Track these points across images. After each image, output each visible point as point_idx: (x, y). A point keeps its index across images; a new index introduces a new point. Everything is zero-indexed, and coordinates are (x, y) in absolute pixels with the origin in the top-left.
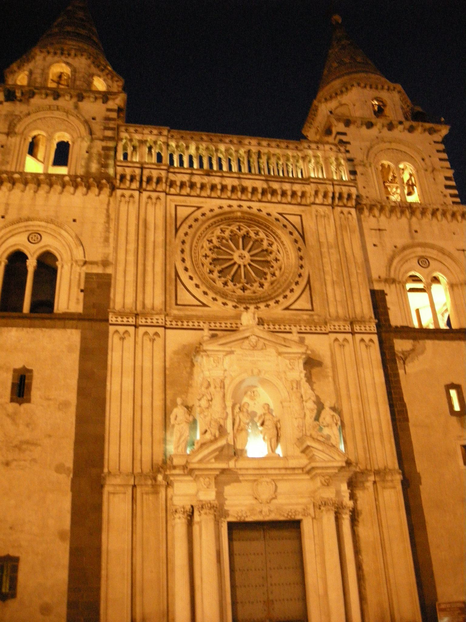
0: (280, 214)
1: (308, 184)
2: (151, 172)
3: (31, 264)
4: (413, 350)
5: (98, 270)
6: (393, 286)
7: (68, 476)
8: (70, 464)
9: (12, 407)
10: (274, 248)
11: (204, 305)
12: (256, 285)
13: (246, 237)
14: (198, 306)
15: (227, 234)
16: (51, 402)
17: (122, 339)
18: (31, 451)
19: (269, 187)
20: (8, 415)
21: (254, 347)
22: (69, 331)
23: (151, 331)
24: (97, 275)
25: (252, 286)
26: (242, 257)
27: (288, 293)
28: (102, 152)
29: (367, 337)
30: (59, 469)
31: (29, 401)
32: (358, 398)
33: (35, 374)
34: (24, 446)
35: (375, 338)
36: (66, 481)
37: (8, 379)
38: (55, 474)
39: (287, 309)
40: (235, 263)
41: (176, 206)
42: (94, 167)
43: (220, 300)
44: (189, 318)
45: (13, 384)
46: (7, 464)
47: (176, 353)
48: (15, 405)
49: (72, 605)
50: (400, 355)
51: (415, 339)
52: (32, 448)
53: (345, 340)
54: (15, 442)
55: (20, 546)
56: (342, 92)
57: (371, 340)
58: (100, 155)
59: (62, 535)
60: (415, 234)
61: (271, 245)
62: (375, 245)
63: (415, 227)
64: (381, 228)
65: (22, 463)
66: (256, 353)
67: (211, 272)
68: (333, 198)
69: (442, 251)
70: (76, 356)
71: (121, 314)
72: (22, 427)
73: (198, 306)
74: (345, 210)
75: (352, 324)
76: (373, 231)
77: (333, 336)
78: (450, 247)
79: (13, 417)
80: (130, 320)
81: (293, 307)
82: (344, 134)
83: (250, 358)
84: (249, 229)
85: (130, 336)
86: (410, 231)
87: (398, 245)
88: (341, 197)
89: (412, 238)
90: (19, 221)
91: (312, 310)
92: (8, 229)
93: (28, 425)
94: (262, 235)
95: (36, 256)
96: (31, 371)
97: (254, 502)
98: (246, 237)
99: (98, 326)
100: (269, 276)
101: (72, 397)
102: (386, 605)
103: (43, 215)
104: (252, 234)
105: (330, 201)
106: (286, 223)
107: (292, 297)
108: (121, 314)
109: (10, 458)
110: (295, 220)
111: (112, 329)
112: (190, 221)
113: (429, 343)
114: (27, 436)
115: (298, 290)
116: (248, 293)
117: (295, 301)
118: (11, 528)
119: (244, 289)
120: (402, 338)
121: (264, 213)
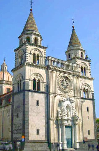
8: (44, 116)
21: (68, 101)
30: (43, 116)
31: (39, 106)
37: (36, 102)
46: (37, 115)
79: (37, 108)
103: (38, 72)
107: (71, 92)
111: (50, 95)
119: (65, 89)
121: (68, 76)
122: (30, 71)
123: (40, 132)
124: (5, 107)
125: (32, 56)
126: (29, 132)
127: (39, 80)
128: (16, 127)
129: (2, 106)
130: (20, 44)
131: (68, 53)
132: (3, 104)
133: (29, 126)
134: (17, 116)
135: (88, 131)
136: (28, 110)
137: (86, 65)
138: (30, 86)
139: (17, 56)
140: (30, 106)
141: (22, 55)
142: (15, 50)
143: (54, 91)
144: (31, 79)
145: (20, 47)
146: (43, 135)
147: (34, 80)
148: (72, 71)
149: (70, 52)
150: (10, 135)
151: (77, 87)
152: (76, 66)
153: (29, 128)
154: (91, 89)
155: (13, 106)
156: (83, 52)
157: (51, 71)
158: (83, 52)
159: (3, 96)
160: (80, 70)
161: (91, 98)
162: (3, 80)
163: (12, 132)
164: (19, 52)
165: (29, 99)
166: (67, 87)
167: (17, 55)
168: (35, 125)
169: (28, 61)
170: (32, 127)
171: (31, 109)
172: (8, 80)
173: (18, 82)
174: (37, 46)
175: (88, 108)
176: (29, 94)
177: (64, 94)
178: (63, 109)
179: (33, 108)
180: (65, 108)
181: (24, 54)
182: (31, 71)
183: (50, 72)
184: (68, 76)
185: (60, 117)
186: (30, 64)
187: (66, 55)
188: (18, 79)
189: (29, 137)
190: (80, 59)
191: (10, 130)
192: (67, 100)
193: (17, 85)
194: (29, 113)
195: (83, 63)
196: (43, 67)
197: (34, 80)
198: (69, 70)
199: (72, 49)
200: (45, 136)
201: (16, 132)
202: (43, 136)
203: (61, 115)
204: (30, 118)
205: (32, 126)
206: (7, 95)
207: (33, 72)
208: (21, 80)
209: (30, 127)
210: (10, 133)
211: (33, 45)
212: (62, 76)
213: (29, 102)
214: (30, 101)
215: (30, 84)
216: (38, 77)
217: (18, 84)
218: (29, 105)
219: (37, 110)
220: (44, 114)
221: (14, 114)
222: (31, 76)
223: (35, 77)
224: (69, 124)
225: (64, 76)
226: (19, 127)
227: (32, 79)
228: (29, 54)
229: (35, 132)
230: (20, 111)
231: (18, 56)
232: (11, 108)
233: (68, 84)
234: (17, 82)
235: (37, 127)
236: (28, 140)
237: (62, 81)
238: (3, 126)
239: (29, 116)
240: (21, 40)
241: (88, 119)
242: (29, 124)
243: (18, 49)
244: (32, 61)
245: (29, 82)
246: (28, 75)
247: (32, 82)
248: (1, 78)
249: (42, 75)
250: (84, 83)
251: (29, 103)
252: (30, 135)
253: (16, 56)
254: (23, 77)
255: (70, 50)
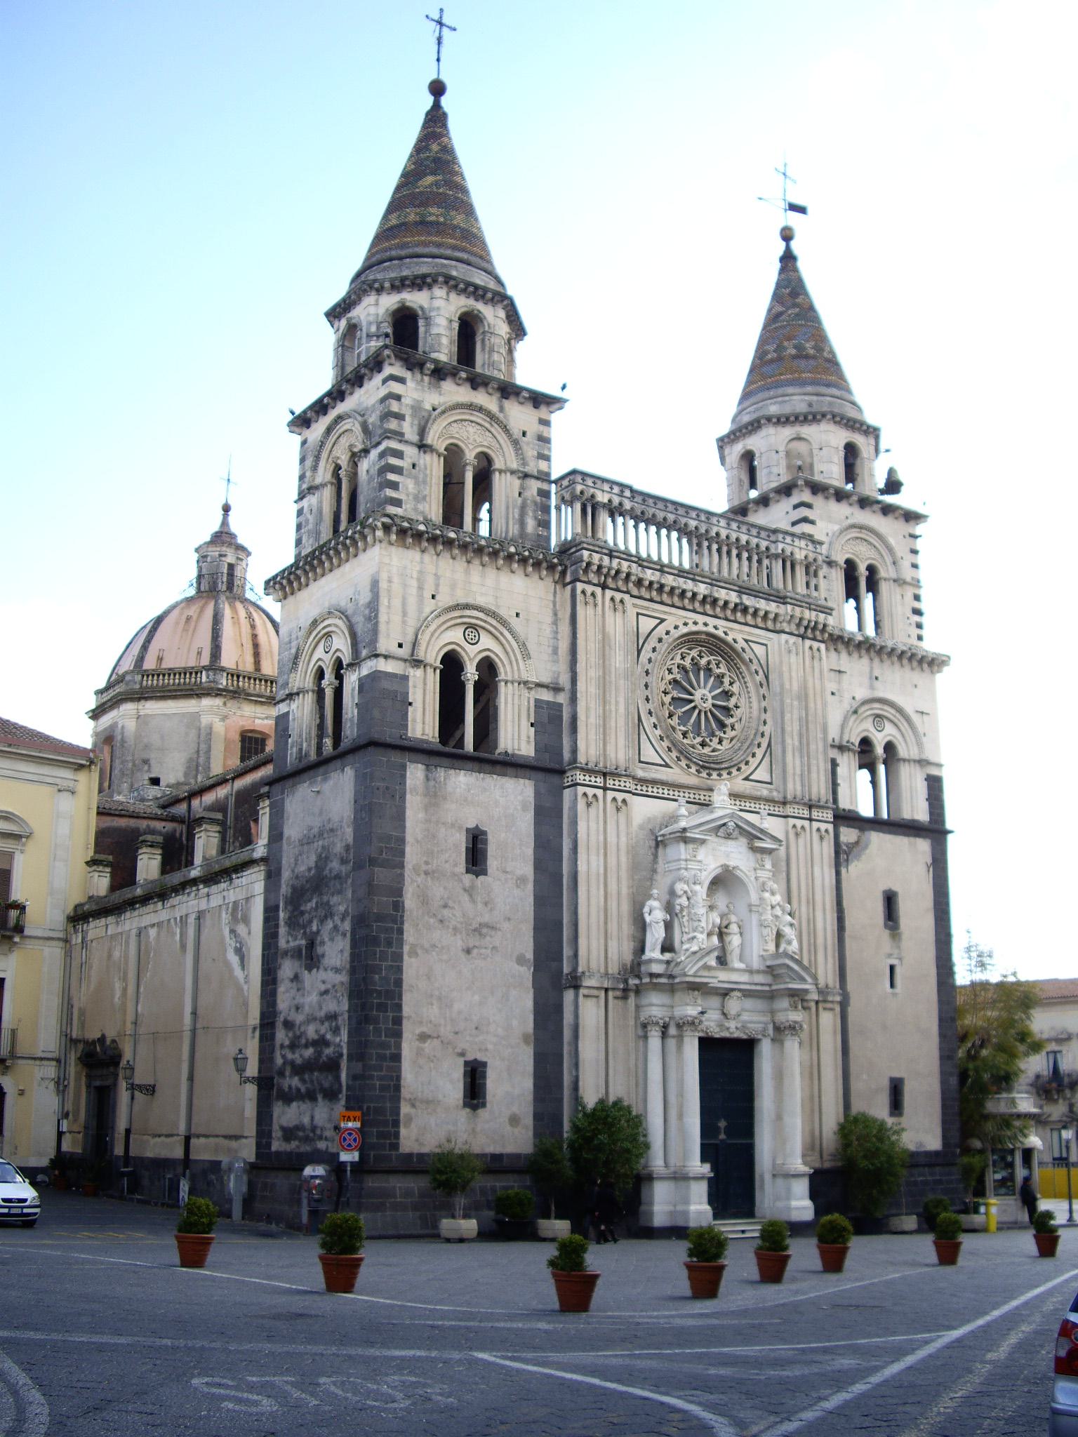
0: (746, 641)
1: (784, 603)
2: (619, 563)
3: (471, 674)
4: (857, 843)
5: (546, 696)
6: (846, 755)
7: (529, 969)
8: (530, 955)
9: (468, 878)
10: (735, 688)
11: (667, 766)
12: (716, 740)
13: (708, 670)
14: (661, 765)
15: (687, 663)
16: (509, 876)
17: (589, 805)
18: (491, 936)
19: (741, 604)
20: (465, 890)
21: (728, 836)
22: (522, 781)
23: (620, 796)
24: (548, 703)
25: (711, 740)
26: (704, 699)
27: (750, 758)
28: (538, 499)
29: (823, 826)
30: (521, 960)
32: (808, 902)
33: (490, 837)
34: (484, 931)
35: (830, 827)
36: (527, 973)
37: (461, 841)
38: (517, 967)
39: (746, 779)
40: (695, 708)
41: (638, 614)
42: (531, 525)
43: (683, 763)
44: (654, 782)
45: (467, 848)
47: (641, 827)
48: (470, 876)
49: (537, 1117)
50: (845, 848)
51: (862, 830)
52: (493, 933)
53: (803, 827)
54: (475, 925)
55: (486, 1050)
56: (806, 419)
57: (827, 831)
58: (535, 503)
59: (525, 1038)
60: (875, 682)
61: (731, 684)
62: (833, 694)
63: (876, 673)
64: (842, 669)
65: (483, 951)
66: (730, 842)
67: (670, 716)
68: (806, 628)
69: (900, 711)
70: (530, 816)
71: (587, 770)
72: (480, 906)
73: (661, 765)
74: (816, 645)
75: (810, 807)
76: (833, 673)
77: (792, 821)
78: (909, 709)
79: (470, 891)
80: (598, 780)
81: (751, 778)
82: (809, 506)
83: (723, 848)
84: (712, 658)
85: (597, 800)
86: (871, 678)
87: (857, 698)
88: (814, 629)
89: (872, 687)
90: (457, 607)
91: (770, 783)
92: (442, 619)
93: (486, 904)
94: (723, 669)
95: (475, 664)
96: (484, 833)
97: (722, 1017)
98: (720, 677)
99: (555, 779)
100: (728, 729)
101: (528, 870)
102: (817, 1133)
103: (481, 601)
104: (726, 680)
105: (802, 630)
106: (752, 657)
107: (754, 762)
108: (587, 770)
109: (471, 945)
110: (759, 650)
112: (652, 642)
113: (876, 839)
114: (486, 918)
115: (759, 753)
116: (706, 750)
117: (756, 769)
118: (477, 1028)
119: (703, 744)
120: (848, 826)
121: (729, 639)
122: (414, 583)
123: (494, 1085)
124: (211, 878)
125: (434, 468)
126: (398, 1088)
127: (488, 668)
128: (293, 1046)
129: (194, 873)
130: (341, 365)
131: (739, 448)
132: (198, 859)
133: (398, 1035)
134: (310, 957)
135: (886, 1084)
136: (398, 906)
137: (890, 549)
138: (415, 714)
139: (315, 468)
140: (408, 872)
141: (354, 455)
142: (302, 422)
143: (619, 754)
144: (420, 654)
145: (337, 394)
146: (515, 1109)
147: (451, 664)
148: (768, 597)
149: (754, 442)
150: (250, 1111)
151: (805, 722)
152: (800, 551)
153: (397, 1058)
154: (920, 744)
155: (273, 877)
156: (859, 440)
157: (589, 589)
158: (859, 440)
159: (209, 798)
160: (833, 583)
161: (921, 813)
162: (214, 665)
163: (267, 1087)
164: (329, 431)
165: (400, 817)
166: (722, 725)
167: (317, 458)
168: (446, 1031)
169: (397, 503)
170: (427, 1046)
171: (424, 900)
172: (248, 666)
173: (320, 674)
174: (476, 382)
175: (890, 900)
176: (404, 777)
177: (692, 780)
178: (684, 901)
179: (437, 891)
180: (701, 891)
181: (366, 451)
182: (420, 588)
183: (580, 597)
184: (736, 634)
185: (657, 968)
186: (418, 536)
187: (723, 460)
188: (320, 652)
189: (396, 1123)
190: (840, 496)
191: (252, 1069)
192: (719, 829)
193: (309, 700)
194: (401, 931)
195: (861, 527)
196: (523, 561)
197: (451, 664)
198: (742, 590)
199: (769, 419)
200: (529, 1120)
201: (295, 1082)
202: (514, 1120)
203: (667, 947)
204: (411, 968)
205: (423, 1037)
206: (240, 784)
207: (445, 600)
208: (339, 665)
209: (408, 1049)
210: (251, 1090)
211: (439, 373)
212: (684, 630)
213: (402, 841)
214: (409, 838)
215: (415, 695)
216: (483, 634)
217: (320, 694)
218: (402, 866)
219: (467, 904)
220: (526, 945)
221: (285, 940)
222: (424, 639)
223: (456, 635)
224: (732, 1025)
225: (691, 640)
226: (321, 1042)
227: (433, 654)
228: (410, 452)
229: (452, 1088)
230: (329, 914)
231: (322, 464)
232: (259, 887)
233: (733, 701)
234: (309, 682)
235: (462, 1045)
236: (396, 1146)
237: (681, 688)
238: (194, 1031)
239: (399, 957)
240: (350, 335)
241: (892, 985)
242: (398, 1021)
243: (320, 407)
244: (434, 510)
245: (405, 678)
246: (397, 619)
247: (433, 680)
248: (194, 654)
249: (514, 622)
250: (862, 693)
251: (402, 853)
252: (405, 1109)
253: (309, 462)
254: (353, 635)
255: (753, 427)
